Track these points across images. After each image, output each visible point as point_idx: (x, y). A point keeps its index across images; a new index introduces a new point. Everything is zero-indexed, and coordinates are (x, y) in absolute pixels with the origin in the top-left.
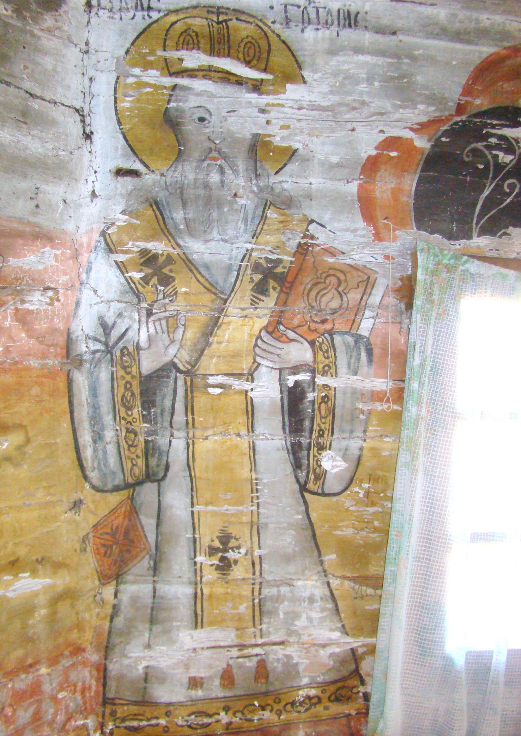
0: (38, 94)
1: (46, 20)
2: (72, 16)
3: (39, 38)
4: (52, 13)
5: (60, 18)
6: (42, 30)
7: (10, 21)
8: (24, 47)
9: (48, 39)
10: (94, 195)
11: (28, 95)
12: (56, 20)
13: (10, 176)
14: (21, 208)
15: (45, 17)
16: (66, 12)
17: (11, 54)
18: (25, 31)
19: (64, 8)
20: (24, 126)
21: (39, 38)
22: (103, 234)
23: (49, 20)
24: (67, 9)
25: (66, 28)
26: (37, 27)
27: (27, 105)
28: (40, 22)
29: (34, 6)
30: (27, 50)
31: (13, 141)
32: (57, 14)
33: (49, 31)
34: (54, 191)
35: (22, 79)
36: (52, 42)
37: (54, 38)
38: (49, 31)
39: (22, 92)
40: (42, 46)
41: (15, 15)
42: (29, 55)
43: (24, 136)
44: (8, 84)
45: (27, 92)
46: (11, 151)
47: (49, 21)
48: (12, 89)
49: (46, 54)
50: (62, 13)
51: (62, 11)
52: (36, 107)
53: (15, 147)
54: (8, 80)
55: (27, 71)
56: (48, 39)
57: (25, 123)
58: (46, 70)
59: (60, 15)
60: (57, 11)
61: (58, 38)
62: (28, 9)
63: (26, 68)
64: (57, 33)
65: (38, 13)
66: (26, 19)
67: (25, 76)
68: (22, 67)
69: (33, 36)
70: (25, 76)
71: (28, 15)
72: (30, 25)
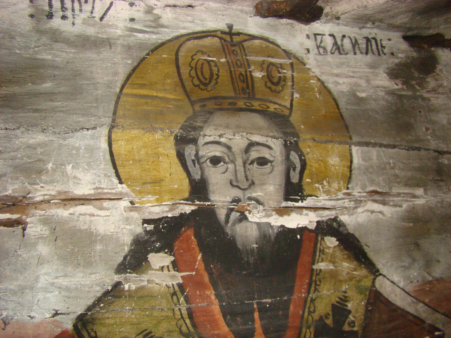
0: (445, 150)
1: (428, 81)
2: (446, 72)
3: (429, 100)
4: (430, 75)
5: (438, 77)
6: (428, 92)
7: (403, 93)
8: (420, 112)
9: (435, 98)
11: (436, 154)
12: (436, 80)
13: (444, 236)
15: (427, 80)
16: (441, 70)
17: (412, 121)
18: (415, 98)
19: (439, 67)
20: (442, 183)
21: (429, 100)
23: (431, 83)
24: (441, 68)
25: (445, 84)
26: (424, 91)
27: (439, 164)
28: (425, 85)
29: (416, 74)
30: (422, 113)
31: (438, 202)
32: (435, 74)
33: (434, 90)
35: (428, 140)
36: (439, 100)
37: (440, 96)
38: (434, 90)
39: (431, 152)
40: (433, 105)
41: (405, 87)
42: (426, 117)
43: (445, 193)
44: (419, 149)
45: (435, 151)
46: (439, 212)
47: (431, 83)
48: (422, 152)
49: (438, 112)
50: (438, 72)
51: (437, 71)
52: (446, 162)
53: (442, 207)
54: (417, 146)
55: (429, 131)
56: (435, 98)
57: (442, 180)
58: (443, 126)
59: (437, 74)
60: (435, 72)
61: (442, 94)
62: (413, 78)
63: (427, 129)
64: (440, 90)
65: (422, 78)
66: (414, 87)
67: (429, 137)
68: (424, 129)
69: (424, 99)
70: (429, 137)
71: (414, 82)
72: (418, 91)
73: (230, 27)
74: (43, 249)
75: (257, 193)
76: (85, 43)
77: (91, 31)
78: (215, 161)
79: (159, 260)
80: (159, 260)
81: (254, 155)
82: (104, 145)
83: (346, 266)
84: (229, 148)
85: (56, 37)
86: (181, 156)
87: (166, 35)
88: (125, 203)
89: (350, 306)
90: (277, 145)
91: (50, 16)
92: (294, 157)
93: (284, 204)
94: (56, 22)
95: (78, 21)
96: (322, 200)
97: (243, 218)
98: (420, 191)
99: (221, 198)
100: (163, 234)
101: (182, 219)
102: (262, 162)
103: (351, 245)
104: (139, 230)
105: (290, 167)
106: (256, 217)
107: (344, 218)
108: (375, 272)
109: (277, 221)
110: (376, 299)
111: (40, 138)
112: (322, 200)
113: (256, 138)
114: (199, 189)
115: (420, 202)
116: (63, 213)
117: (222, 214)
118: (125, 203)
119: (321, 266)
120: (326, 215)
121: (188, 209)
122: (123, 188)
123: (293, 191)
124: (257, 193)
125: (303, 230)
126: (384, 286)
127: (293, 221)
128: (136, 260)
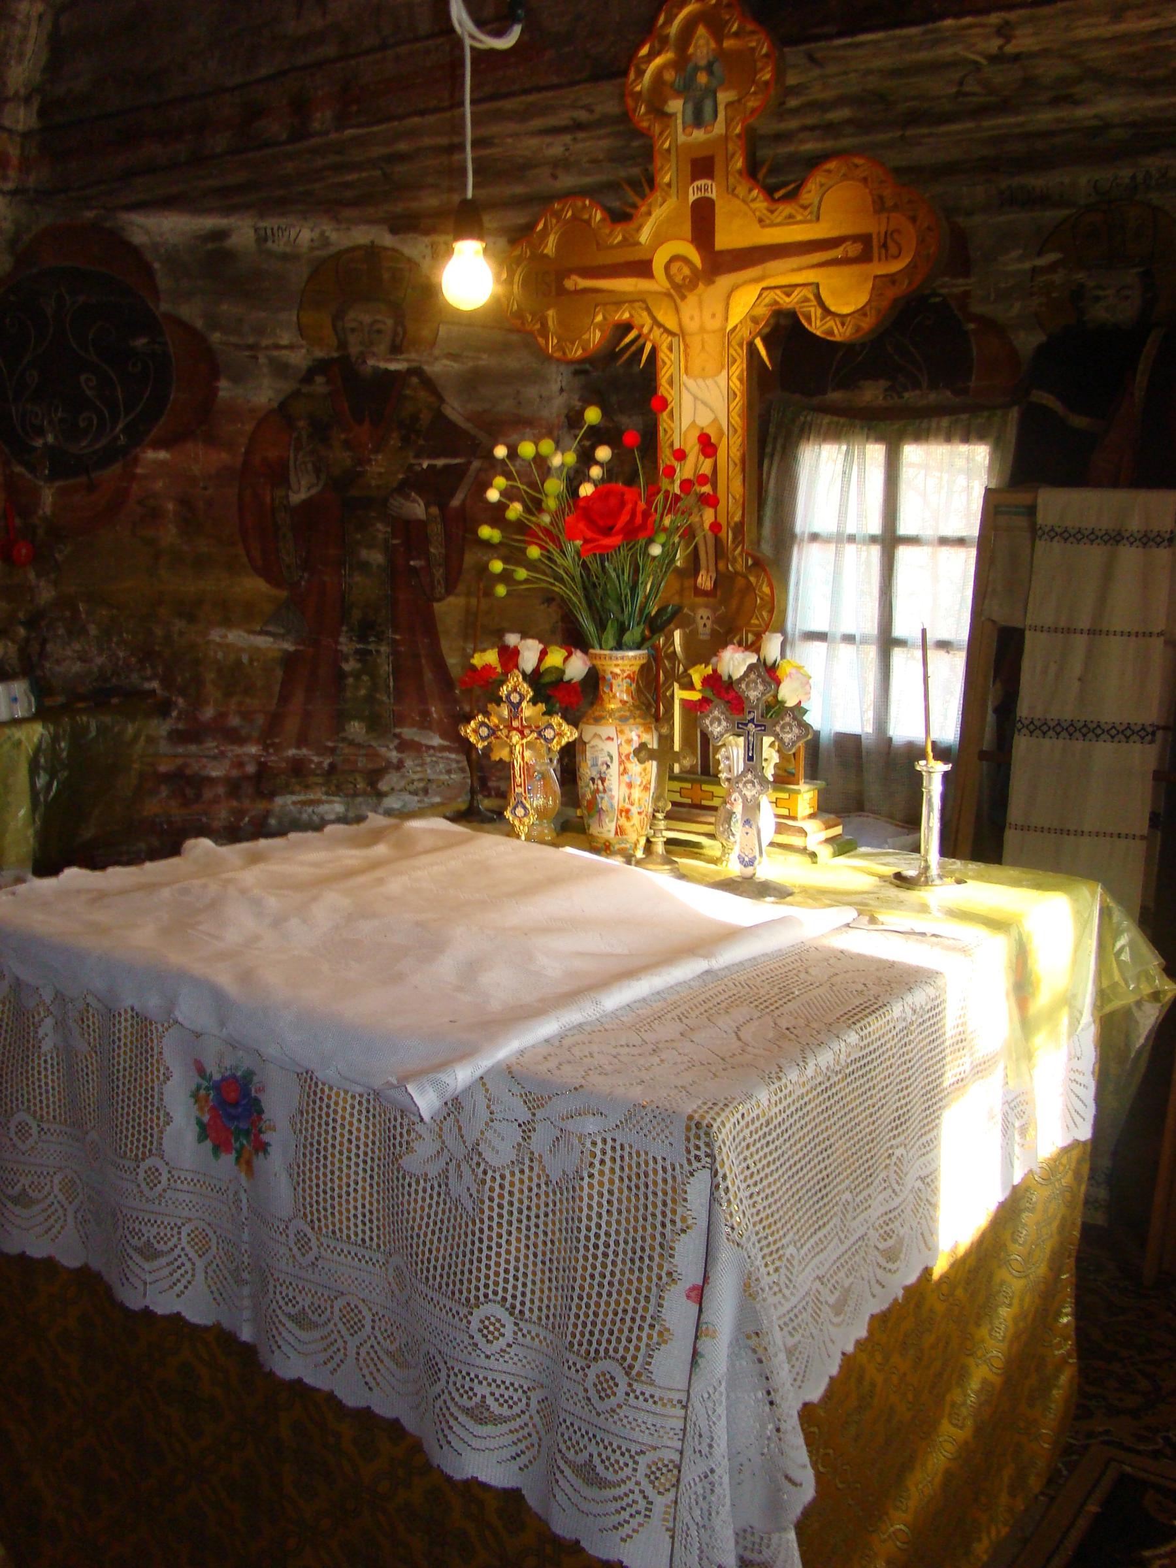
10: (562, 390)
14: (506, 406)
22: (567, 416)
34: (531, 392)
73: (372, 242)
74: (265, 370)
75: (375, 349)
76: (285, 257)
77: (288, 249)
78: (353, 330)
79: (320, 379)
80: (320, 379)
81: (376, 327)
82: (295, 318)
83: (423, 394)
84: (361, 323)
85: (270, 254)
86: (334, 326)
87: (333, 250)
88: (304, 351)
89: (422, 416)
90: (390, 322)
91: (266, 240)
92: (400, 329)
93: (389, 356)
94: (269, 244)
95: (282, 243)
96: (413, 356)
97: (364, 362)
98: (485, 356)
99: (354, 350)
100: (320, 367)
101: (333, 361)
102: (379, 332)
103: (427, 382)
104: (310, 363)
105: (395, 334)
106: (371, 362)
107: (425, 367)
108: (441, 400)
109: (383, 365)
110: (439, 416)
111: (262, 314)
112: (413, 356)
113: (378, 317)
114: (343, 345)
115: (481, 363)
116: (275, 353)
117: (354, 360)
118: (304, 351)
119: (408, 392)
120: (414, 364)
121: (335, 355)
122: (304, 342)
123: (396, 349)
124: (375, 349)
125: (397, 373)
126: (448, 411)
127: (393, 366)
128: (308, 378)
